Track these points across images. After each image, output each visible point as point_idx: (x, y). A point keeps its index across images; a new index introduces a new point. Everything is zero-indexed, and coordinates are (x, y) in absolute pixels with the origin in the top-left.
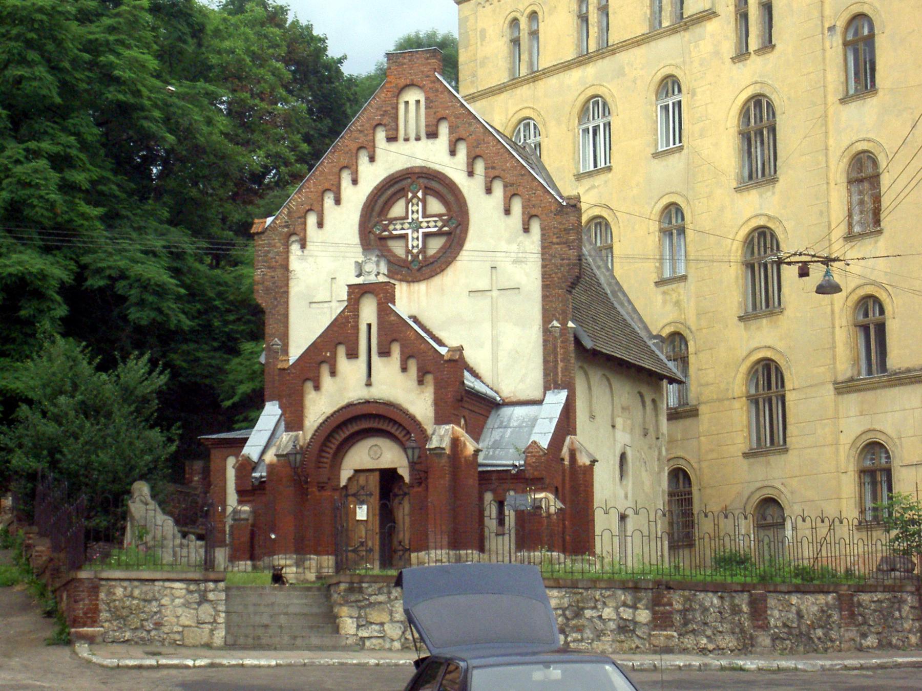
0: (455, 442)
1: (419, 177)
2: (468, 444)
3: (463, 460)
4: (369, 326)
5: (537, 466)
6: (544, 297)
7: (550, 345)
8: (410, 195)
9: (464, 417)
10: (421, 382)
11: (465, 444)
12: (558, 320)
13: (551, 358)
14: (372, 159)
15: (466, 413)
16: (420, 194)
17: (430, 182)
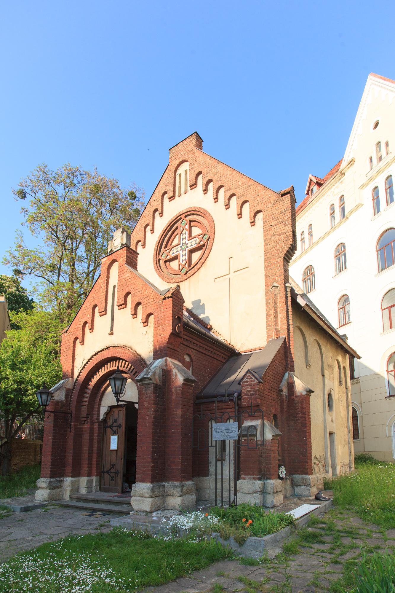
0: (166, 374)
1: (186, 217)
2: (175, 371)
3: (174, 390)
4: (114, 287)
5: (252, 395)
6: (266, 267)
7: (271, 302)
8: (181, 229)
9: (188, 355)
10: (146, 322)
11: (176, 375)
12: (277, 282)
13: (272, 312)
14: (161, 214)
15: (193, 353)
16: (187, 227)
17: (192, 216)
